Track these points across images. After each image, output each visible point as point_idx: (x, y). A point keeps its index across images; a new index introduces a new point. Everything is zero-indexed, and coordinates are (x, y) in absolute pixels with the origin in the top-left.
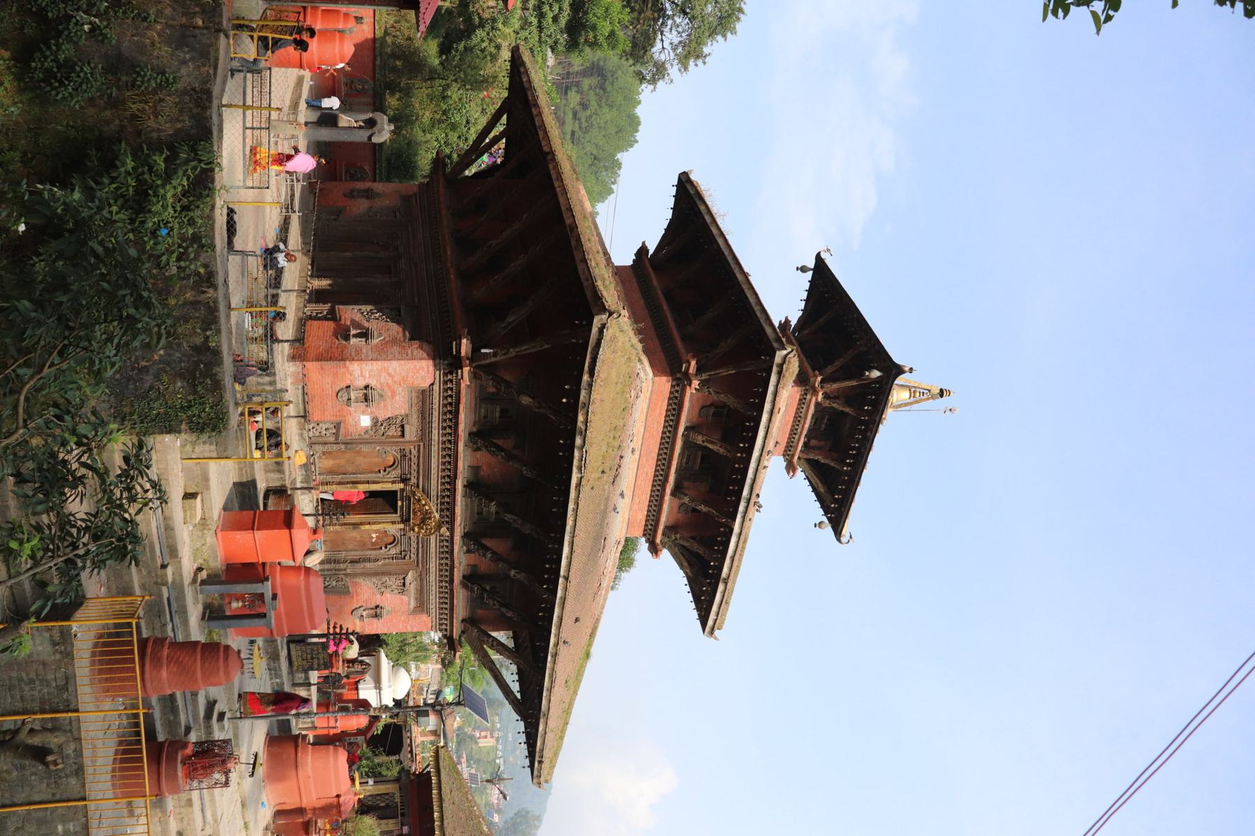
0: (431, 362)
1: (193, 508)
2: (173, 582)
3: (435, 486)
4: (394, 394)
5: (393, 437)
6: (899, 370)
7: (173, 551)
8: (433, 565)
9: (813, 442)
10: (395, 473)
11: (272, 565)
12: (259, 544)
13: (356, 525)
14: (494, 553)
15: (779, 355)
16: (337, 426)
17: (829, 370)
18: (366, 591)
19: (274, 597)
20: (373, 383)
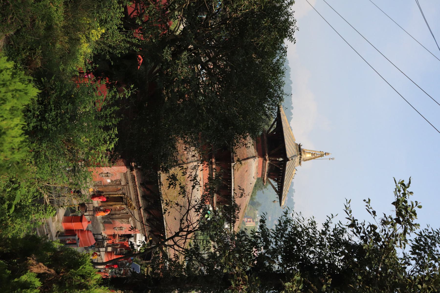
0: (125, 167)
1: (55, 219)
2: (50, 238)
3: (133, 197)
4: (116, 175)
5: (118, 184)
6: (288, 160)
7: (50, 230)
8: (137, 216)
9: (271, 173)
10: (121, 192)
11: (78, 230)
12: (74, 226)
13: (111, 205)
14: (153, 215)
15: (233, 164)
16: (101, 182)
17: (273, 152)
18: (118, 223)
19: (78, 239)
20: (109, 172)
